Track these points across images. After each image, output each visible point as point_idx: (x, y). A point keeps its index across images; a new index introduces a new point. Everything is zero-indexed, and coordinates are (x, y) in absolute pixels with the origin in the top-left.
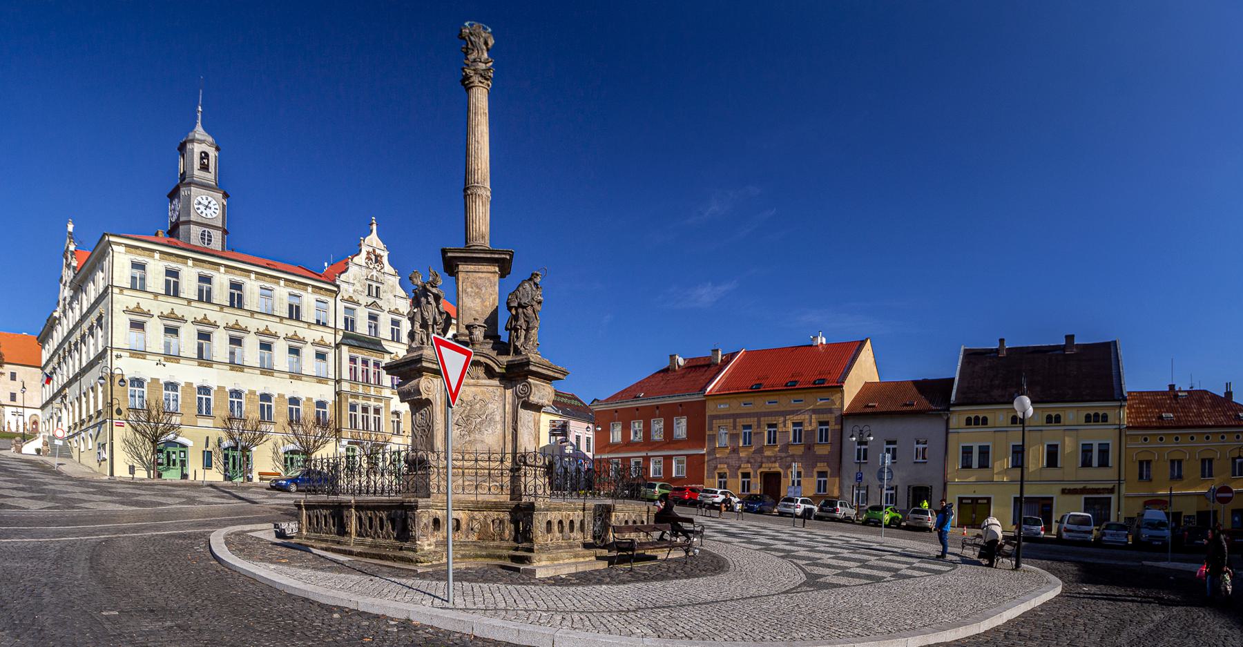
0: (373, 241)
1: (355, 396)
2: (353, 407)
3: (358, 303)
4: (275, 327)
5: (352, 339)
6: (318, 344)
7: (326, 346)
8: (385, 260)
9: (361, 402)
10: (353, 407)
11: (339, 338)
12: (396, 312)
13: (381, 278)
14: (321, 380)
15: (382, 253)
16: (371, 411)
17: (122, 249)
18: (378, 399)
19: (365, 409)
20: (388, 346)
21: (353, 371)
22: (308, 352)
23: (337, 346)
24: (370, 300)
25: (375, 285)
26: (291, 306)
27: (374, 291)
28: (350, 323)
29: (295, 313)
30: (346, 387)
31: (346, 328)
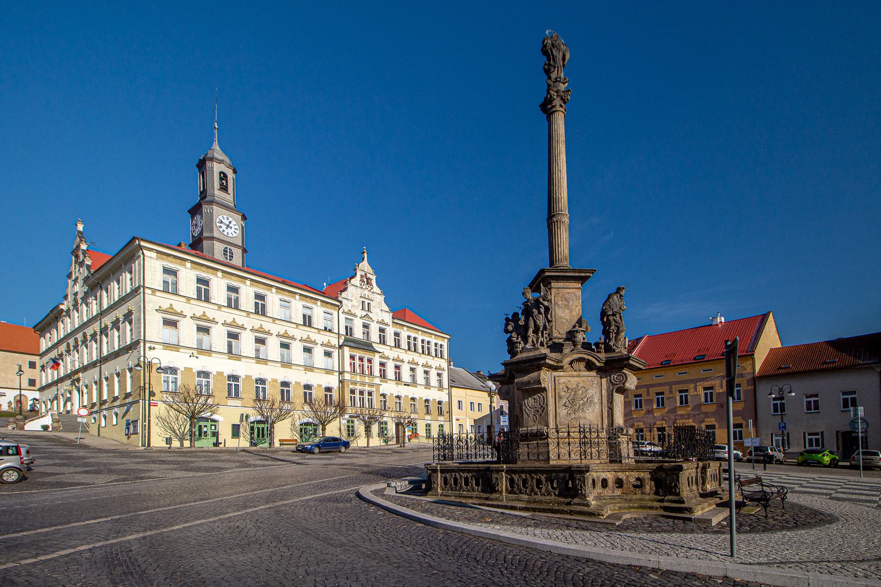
0: (365, 266)
1: (355, 383)
2: (353, 392)
3: (355, 315)
4: (292, 331)
5: (350, 341)
6: (326, 345)
7: (331, 347)
8: (374, 282)
9: (358, 387)
10: (353, 392)
11: (341, 341)
12: (382, 322)
13: (371, 296)
14: (329, 371)
15: (371, 277)
16: (366, 394)
17: (154, 255)
18: (371, 385)
19: (361, 393)
20: (377, 347)
21: (353, 365)
22: (318, 351)
23: (340, 347)
24: (364, 313)
25: (367, 301)
26: (304, 316)
27: (366, 307)
28: (349, 330)
29: (307, 321)
30: (347, 376)
31: (347, 334)
